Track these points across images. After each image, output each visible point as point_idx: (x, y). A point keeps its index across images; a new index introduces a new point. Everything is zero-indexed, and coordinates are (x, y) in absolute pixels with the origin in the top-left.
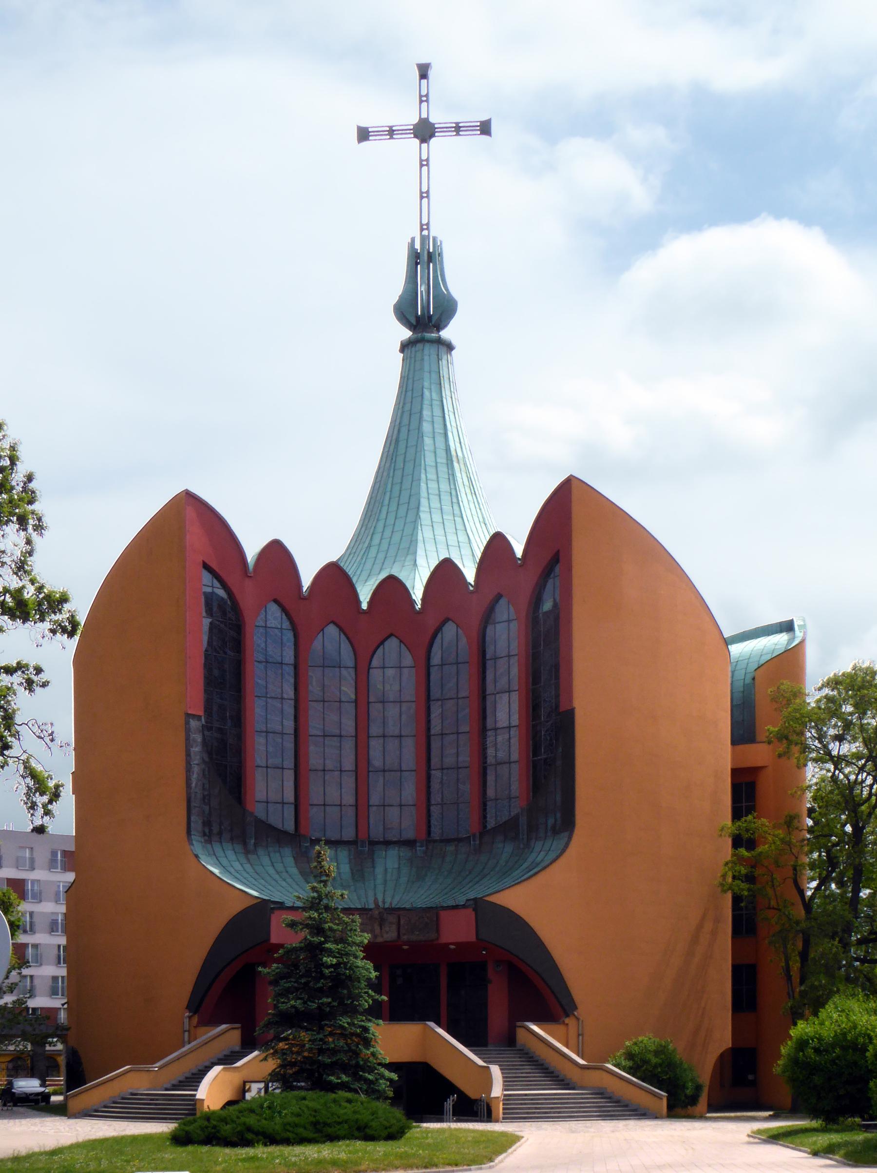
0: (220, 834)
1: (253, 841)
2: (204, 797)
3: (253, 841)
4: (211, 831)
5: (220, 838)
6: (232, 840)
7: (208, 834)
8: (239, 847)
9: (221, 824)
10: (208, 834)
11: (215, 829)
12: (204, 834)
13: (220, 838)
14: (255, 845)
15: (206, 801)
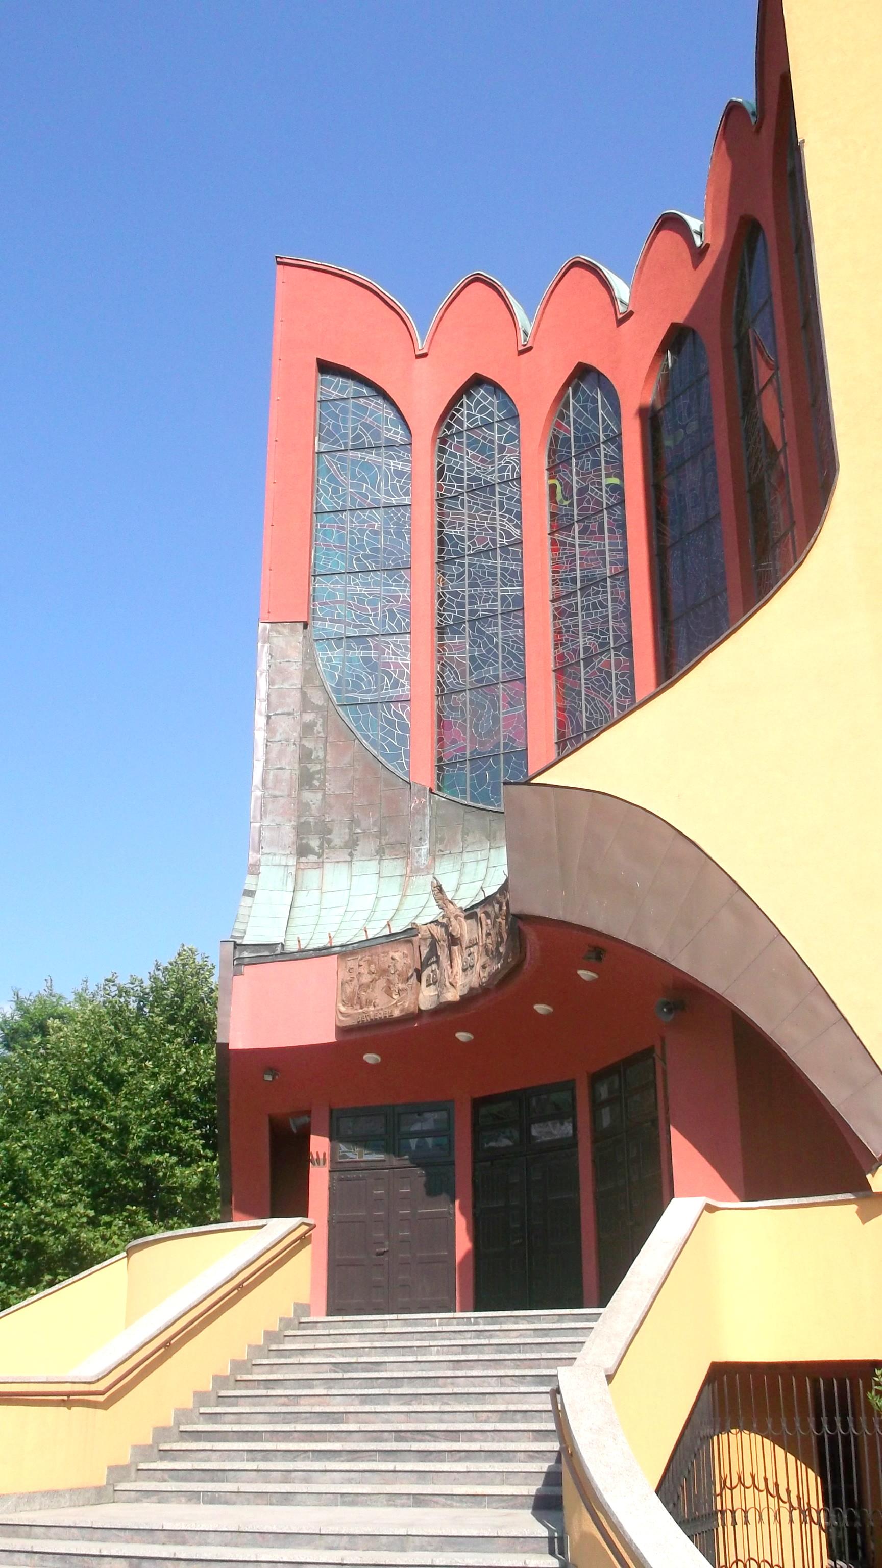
0: (351, 845)
1: (425, 848)
2: (306, 780)
3: (427, 846)
4: (326, 842)
5: (351, 855)
6: (380, 853)
7: (317, 849)
8: (394, 867)
9: (354, 822)
10: (317, 849)
11: (338, 837)
12: (302, 851)
13: (351, 855)
14: (433, 855)
15: (316, 783)
